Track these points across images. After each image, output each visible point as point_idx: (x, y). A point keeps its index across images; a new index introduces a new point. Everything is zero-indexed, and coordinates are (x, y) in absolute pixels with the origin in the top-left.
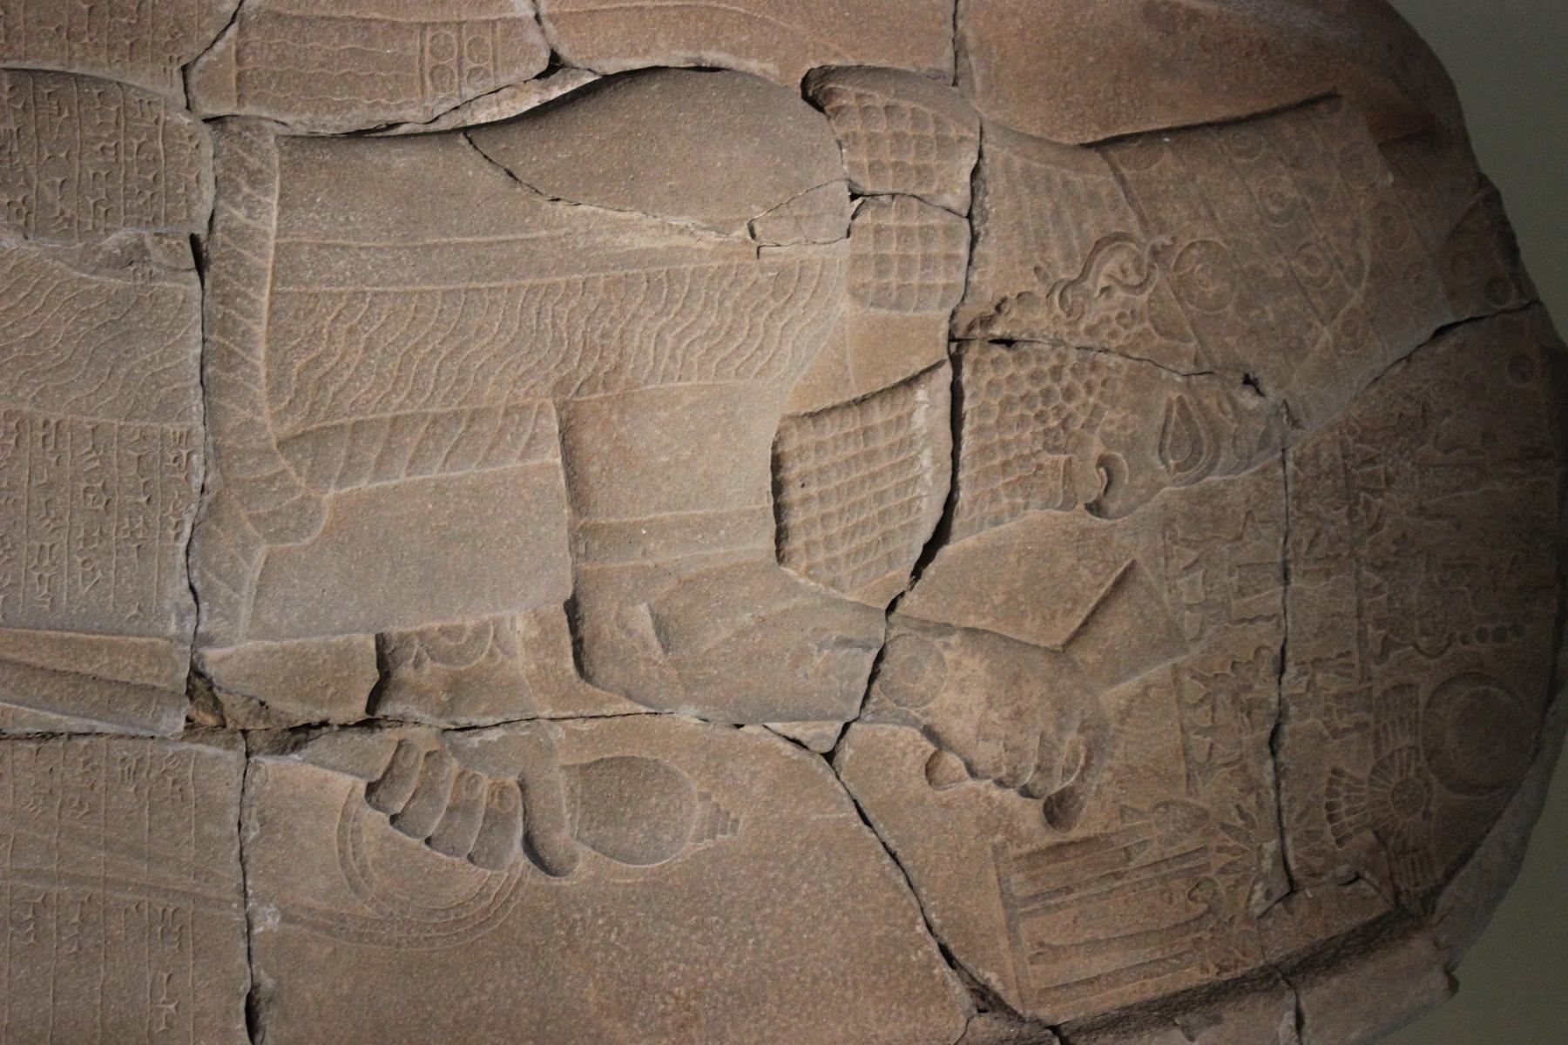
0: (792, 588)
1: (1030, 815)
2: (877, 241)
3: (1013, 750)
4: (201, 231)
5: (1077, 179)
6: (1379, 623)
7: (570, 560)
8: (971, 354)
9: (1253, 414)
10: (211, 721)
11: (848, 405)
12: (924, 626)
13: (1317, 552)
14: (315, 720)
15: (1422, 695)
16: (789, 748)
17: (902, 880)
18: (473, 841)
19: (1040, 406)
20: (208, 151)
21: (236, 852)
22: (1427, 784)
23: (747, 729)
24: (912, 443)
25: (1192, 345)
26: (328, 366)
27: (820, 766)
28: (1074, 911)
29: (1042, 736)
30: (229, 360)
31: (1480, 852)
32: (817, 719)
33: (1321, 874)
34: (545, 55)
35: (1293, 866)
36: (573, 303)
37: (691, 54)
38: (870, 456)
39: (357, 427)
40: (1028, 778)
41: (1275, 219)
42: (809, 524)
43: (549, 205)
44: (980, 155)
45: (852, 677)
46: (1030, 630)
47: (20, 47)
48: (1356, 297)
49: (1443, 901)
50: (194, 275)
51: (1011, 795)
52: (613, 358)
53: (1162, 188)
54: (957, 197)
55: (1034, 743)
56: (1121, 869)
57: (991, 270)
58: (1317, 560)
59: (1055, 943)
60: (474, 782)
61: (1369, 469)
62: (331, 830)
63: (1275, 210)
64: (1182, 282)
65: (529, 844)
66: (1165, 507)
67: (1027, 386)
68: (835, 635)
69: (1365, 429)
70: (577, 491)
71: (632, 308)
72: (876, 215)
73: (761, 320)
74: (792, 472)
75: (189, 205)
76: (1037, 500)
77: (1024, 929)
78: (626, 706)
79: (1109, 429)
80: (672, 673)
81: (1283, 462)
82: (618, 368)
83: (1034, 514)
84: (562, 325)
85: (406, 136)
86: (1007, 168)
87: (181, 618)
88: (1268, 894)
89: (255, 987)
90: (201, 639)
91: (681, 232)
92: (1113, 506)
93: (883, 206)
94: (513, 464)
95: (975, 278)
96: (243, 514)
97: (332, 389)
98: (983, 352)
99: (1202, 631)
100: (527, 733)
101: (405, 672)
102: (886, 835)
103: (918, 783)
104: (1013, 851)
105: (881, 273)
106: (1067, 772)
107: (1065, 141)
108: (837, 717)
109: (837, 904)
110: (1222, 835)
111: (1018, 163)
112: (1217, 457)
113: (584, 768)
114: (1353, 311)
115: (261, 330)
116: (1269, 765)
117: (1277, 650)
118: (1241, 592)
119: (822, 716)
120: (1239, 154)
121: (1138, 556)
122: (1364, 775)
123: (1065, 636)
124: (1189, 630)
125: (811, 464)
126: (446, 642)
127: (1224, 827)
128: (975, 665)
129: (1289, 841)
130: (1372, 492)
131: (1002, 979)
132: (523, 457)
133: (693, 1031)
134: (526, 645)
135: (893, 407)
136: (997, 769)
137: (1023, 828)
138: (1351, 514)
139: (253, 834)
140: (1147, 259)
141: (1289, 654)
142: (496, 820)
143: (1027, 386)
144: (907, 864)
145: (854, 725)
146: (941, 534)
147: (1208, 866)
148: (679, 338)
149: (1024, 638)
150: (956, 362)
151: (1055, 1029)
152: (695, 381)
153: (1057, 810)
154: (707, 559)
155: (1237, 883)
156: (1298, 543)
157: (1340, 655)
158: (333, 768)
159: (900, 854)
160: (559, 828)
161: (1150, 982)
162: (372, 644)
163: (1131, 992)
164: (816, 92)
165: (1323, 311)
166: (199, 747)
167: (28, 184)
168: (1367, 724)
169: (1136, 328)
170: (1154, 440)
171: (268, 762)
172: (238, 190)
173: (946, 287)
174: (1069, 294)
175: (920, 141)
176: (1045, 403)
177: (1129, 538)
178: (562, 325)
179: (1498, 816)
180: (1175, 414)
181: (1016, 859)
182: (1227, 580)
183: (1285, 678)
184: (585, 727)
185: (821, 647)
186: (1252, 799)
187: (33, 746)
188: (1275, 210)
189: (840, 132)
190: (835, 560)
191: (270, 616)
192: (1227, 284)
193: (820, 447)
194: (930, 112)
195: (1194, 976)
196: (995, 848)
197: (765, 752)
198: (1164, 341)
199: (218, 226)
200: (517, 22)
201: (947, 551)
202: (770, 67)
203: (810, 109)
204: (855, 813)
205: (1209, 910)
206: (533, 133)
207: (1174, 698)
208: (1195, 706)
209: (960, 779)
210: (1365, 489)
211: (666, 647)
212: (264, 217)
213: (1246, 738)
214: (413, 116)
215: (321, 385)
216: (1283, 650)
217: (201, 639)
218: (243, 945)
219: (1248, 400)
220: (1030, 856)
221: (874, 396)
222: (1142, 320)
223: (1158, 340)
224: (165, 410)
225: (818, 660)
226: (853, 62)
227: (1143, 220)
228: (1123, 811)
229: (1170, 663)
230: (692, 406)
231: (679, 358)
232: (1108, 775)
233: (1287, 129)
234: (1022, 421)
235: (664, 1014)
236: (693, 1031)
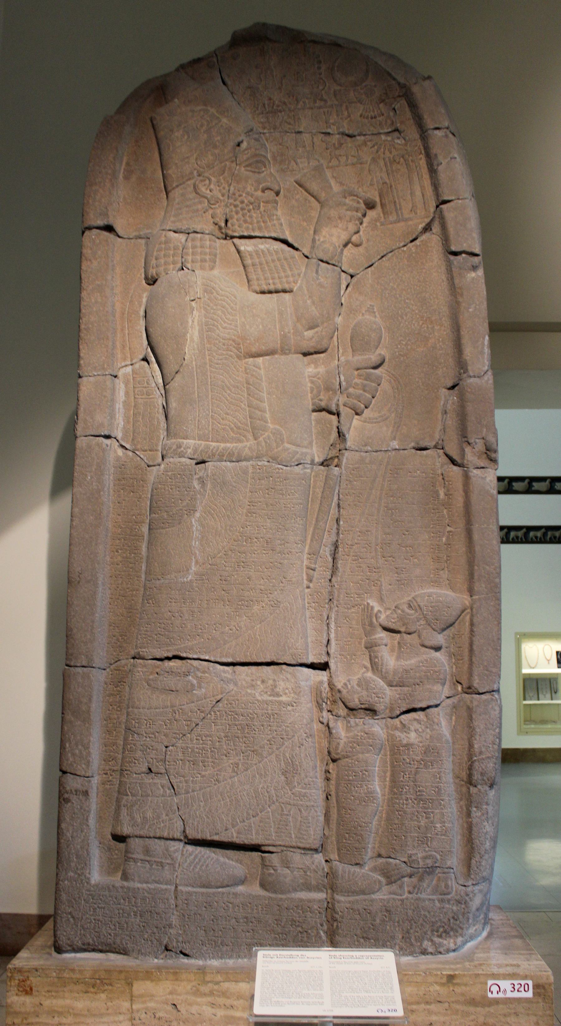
0: (300, 288)
1: (371, 214)
2: (196, 262)
3: (351, 219)
4: (194, 462)
5: (177, 200)
6: (315, 102)
7: (291, 355)
8: (230, 233)
9: (248, 144)
10: (336, 460)
11: (245, 271)
12: (313, 247)
13: (292, 122)
14: (337, 430)
15: (338, 88)
16: (349, 289)
17: (390, 254)
18: (374, 384)
19: (246, 211)
20: (171, 460)
21: (374, 453)
22: (366, 86)
23: (343, 302)
24: (257, 251)
25: (228, 163)
26: (233, 426)
27: (355, 279)
28: (402, 200)
29: (347, 210)
30: (231, 454)
31: (388, 69)
35: (390, 130)
36: (214, 354)
37: (141, 319)
38: (261, 264)
39: (250, 417)
40: (360, 215)
41: (189, 137)
42: (281, 283)
43: (186, 362)
44: (170, 230)
45: (327, 269)
46: (315, 214)
47: (143, 512)
48: (213, 110)
49: (402, 81)
50: (207, 464)
51: (366, 220)
52: (231, 342)
54: (182, 237)
55: (349, 213)
57: (205, 227)
58: (295, 122)
59: (411, 206)
60: (356, 384)
61: (266, 106)
62: (369, 426)
63: (186, 137)
64: (208, 166)
66: (278, 171)
67: (240, 215)
68: (314, 275)
70: (271, 353)
71: (216, 336)
72: (188, 262)
73: (219, 298)
74: (265, 288)
75: (187, 465)
76: (275, 212)
77: (406, 216)
79: (253, 189)
80: (325, 324)
81: (264, 134)
82: (234, 341)
83: (279, 213)
84: (221, 357)
85: (166, 403)
86: (174, 222)
87: (305, 468)
88: (398, 138)
89: (414, 448)
90: (312, 463)
91: (193, 322)
92: (277, 188)
93: (185, 260)
94: (262, 372)
95: (207, 232)
96: (276, 450)
97: (239, 424)
98: (229, 229)
99: (316, 159)
101: (323, 404)
102: (376, 259)
103: (361, 249)
104: (382, 219)
105: (205, 261)
106: (358, 202)
107: (166, 204)
108: (340, 275)
109: (397, 274)
110: (379, 153)
111: (172, 219)
112: (262, 155)
113: (353, 351)
114: (217, 112)
115: (222, 445)
116: (358, 138)
117: (322, 135)
118: (304, 147)
119: (340, 279)
120: (169, 148)
121: (292, 180)
122: (362, 107)
123: (316, 203)
125: (263, 282)
127: (377, 152)
128: (325, 231)
129: (382, 131)
130: (274, 104)
131: (421, 223)
132: (260, 369)
133: (433, 318)
135: (246, 257)
136: (357, 224)
137: (375, 216)
138: (280, 111)
139: (369, 448)
140: (201, 178)
141: (324, 131)
142: (368, 378)
143: (240, 215)
144: (385, 253)
145: (343, 269)
147: (389, 158)
148: (225, 322)
149: (317, 216)
150: (232, 237)
151: (437, 207)
153: (370, 206)
154: (291, 314)
155: (395, 148)
156: (289, 129)
158: (351, 425)
159: (382, 255)
160: (371, 358)
161: (424, 176)
162: (315, 414)
163: (427, 182)
164: (152, 281)
166: (343, 464)
167: (181, 510)
168: (347, 106)
169: (222, 181)
170: (257, 175)
171: (349, 444)
172: (182, 451)
173: (210, 240)
174: (212, 202)
175: (165, 249)
176: (245, 209)
177: (287, 182)
178: (221, 357)
179: (376, 63)
180: (249, 169)
181: (385, 218)
183: (331, 132)
184: (341, 351)
185: (318, 279)
186: (368, 143)
187: (341, 510)
188: (186, 137)
189: (163, 274)
190: (292, 275)
191: (305, 443)
194: (157, 246)
195: (423, 162)
196: (382, 225)
197: (350, 297)
198: (226, 172)
199: (193, 457)
200: (133, 371)
201: (290, 240)
202: (145, 295)
203: (157, 283)
204: (369, 269)
205: (403, 157)
206: (164, 366)
208: (339, 161)
209: (360, 236)
210: (273, 107)
211: (317, 326)
212: (191, 444)
213: (350, 145)
214: (161, 401)
215: (238, 428)
216: (323, 133)
217: (312, 463)
218: (401, 451)
219: (244, 145)
220: (384, 213)
221: (242, 263)
223: (226, 174)
224: (245, 472)
225: (322, 280)
226: (143, 270)
227: (190, 179)
228: (371, 185)
229: (326, 170)
230: (245, 317)
232: (360, 189)
233: (161, 134)
234: (251, 217)
235: (428, 328)
236: (433, 318)
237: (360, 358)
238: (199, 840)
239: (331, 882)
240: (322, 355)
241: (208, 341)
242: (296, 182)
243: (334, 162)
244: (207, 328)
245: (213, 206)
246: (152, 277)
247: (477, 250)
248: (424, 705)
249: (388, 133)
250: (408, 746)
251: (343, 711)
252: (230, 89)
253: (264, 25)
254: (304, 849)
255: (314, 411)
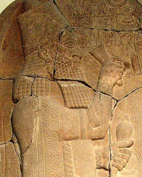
0: (91, 106)
1: (128, 70)
8: (56, 77)
9: (66, 32)
12: (98, 86)
17: (137, 90)
26: (56, 175)
32: (111, 103)
33: (139, 25)
34: (10, 142)
44: (26, 76)
51: (125, 73)
52: (55, 133)
53: (31, 47)
54: (32, 79)
56: (136, 56)
58: (90, 24)
64: (45, 44)
65: (128, 147)
67: (61, 69)
69: (70, 15)
76: (79, 68)
78: (108, 132)
82: (57, 132)
83: (81, 68)
92: (80, 56)
94: (71, 148)
100: (112, 147)
101: (102, 165)
102: (130, 93)
103: (122, 87)
104: (133, 73)
106: (121, 64)
111: (27, 70)
112: (73, 39)
116: (121, 32)
124: (100, 44)
126: (98, 159)
134: (99, 147)
140: (42, 49)
142: (124, 152)
143: (61, 69)
146: (84, 83)
148: (53, 122)
152: (59, 120)
153: (127, 65)
157: (105, 20)
164: (16, 101)
165: (50, 22)
169: (53, 51)
182: (92, 38)
192: (46, 37)
193: (70, 101)
201: (87, 82)
202: (12, 108)
207: (110, 47)
210: (79, 15)
211: (100, 125)
219: (64, 34)
222: (51, 50)
229: (105, 47)
231: (56, 122)
237: (121, 142)
240: (102, 140)
241: (44, 132)
242: (90, 53)
243: (109, 44)
244: (43, 125)
245: (48, 64)
246: (16, 99)
252: (57, 6)
255: (97, 168)
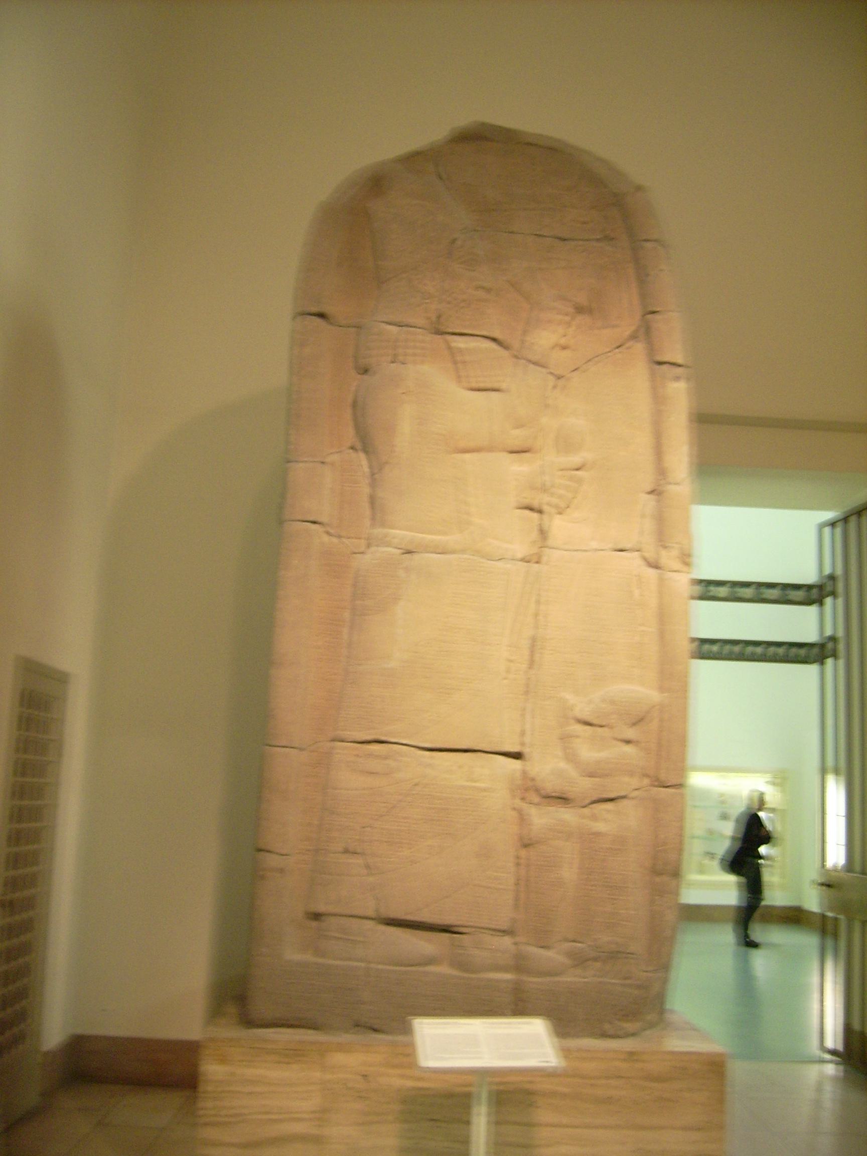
65: (577, 469)
101: (527, 502)
146: (494, 340)
151: (644, 315)
219: (459, 243)
238: (393, 920)
239: (520, 965)
247: (680, 360)
248: (612, 796)
249: (598, 240)
250: (598, 834)
251: (536, 799)
253: (483, 124)
254: (494, 930)
